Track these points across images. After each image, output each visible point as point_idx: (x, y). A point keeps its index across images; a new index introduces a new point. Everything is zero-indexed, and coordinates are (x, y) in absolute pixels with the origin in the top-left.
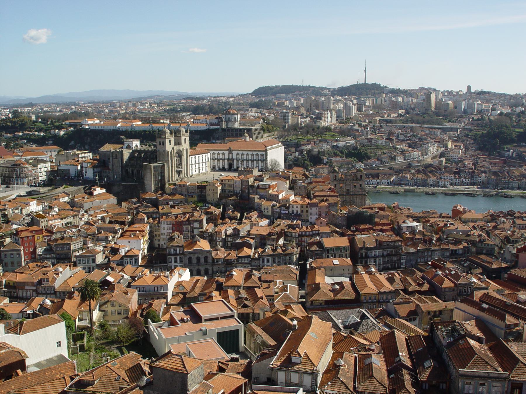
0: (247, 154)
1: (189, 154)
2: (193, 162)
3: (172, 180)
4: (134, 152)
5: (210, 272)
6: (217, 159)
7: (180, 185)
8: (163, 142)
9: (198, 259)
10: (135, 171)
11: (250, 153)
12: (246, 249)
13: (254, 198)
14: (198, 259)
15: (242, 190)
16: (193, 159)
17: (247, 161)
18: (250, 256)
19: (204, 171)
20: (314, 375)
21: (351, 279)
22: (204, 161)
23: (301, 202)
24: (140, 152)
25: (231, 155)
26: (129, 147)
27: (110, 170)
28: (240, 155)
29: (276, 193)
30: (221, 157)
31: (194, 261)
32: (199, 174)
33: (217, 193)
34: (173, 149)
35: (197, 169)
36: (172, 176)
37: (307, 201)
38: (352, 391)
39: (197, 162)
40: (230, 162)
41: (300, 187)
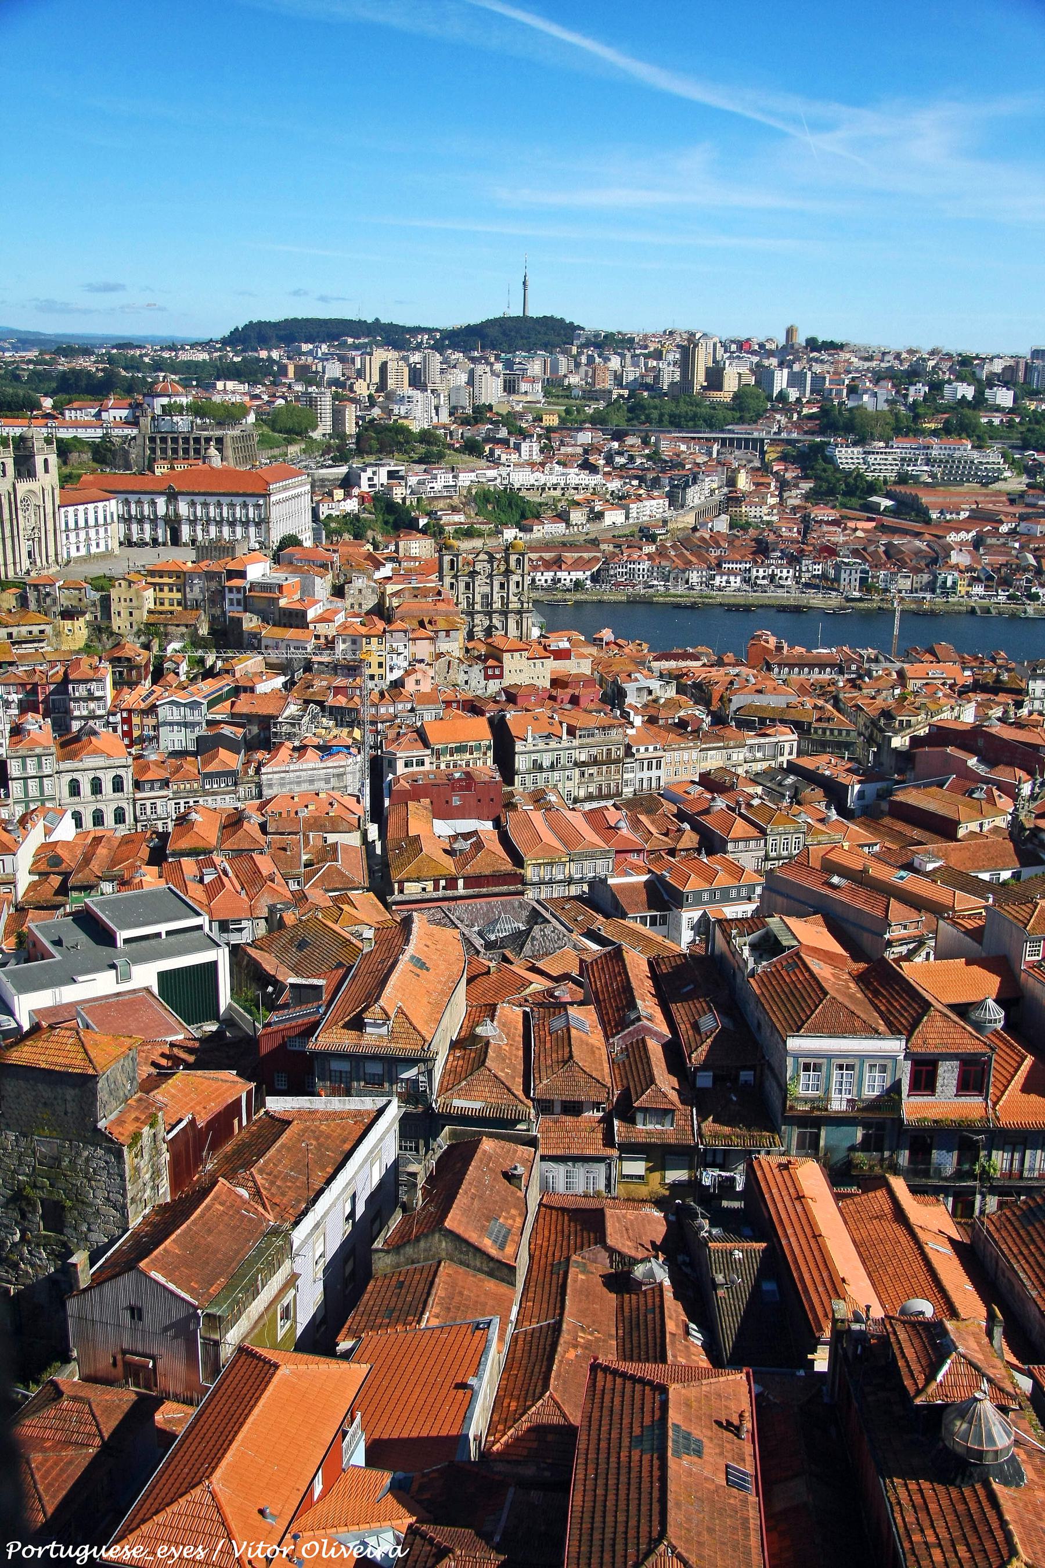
1: (57, 503)
2: (72, 525)
5: (129, 818)
7: (36, 587)
9: (96, 787)
12: (223, 754)
13: (239, 621)
14: (96, 787)
18: (233, 773)
19: (102, 548)
20: (425, 1060)
21: (498, 824)
22: (101, 521)
29: (298, 606)
31: (86, 788)
32: (89, 558)
35: (81, 545)
36: (15, 564)
37: (381, 625)
38: (522, 1097)
39: (82, 524)
41: (360, 591)
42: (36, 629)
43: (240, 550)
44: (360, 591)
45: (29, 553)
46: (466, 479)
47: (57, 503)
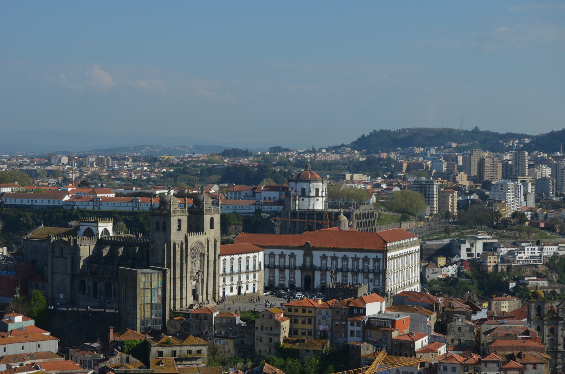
0: (345, 258)
1: (218, 252)
2: (228, 270)
3: (181, 307)
4: (101, 243)
6: (279, 267)
7: (197, 316)
8: (164, 223)
10: (101, 286)
11: (350, 255)
13: (358, 349)
15: (331, 330)
16: (225, 262)
17: (345, 272)
19: (250, 290)
22: (251, 268)
23: (461, 359)
24: (114, 244)
25: (308, 259)
26: (90, 233)
27: (47, 281)
28: (329, 260)
29: (407, 338)
30: (287, 264)
33: (279, 335)
34: (186, 238)
36: (181, 298)
37: (476, 357)
39: (236, 270)
40: (305, 273)
41: (460, 329)
42: (194, 349)
43: (362, 291)
44: (460, 329)
45: (194, 291)
46: (549, 250)
47: (218, 252)
